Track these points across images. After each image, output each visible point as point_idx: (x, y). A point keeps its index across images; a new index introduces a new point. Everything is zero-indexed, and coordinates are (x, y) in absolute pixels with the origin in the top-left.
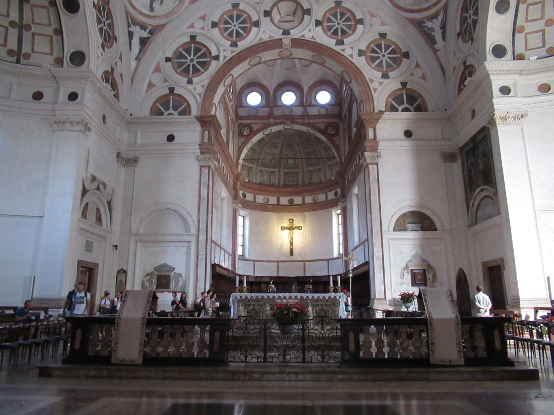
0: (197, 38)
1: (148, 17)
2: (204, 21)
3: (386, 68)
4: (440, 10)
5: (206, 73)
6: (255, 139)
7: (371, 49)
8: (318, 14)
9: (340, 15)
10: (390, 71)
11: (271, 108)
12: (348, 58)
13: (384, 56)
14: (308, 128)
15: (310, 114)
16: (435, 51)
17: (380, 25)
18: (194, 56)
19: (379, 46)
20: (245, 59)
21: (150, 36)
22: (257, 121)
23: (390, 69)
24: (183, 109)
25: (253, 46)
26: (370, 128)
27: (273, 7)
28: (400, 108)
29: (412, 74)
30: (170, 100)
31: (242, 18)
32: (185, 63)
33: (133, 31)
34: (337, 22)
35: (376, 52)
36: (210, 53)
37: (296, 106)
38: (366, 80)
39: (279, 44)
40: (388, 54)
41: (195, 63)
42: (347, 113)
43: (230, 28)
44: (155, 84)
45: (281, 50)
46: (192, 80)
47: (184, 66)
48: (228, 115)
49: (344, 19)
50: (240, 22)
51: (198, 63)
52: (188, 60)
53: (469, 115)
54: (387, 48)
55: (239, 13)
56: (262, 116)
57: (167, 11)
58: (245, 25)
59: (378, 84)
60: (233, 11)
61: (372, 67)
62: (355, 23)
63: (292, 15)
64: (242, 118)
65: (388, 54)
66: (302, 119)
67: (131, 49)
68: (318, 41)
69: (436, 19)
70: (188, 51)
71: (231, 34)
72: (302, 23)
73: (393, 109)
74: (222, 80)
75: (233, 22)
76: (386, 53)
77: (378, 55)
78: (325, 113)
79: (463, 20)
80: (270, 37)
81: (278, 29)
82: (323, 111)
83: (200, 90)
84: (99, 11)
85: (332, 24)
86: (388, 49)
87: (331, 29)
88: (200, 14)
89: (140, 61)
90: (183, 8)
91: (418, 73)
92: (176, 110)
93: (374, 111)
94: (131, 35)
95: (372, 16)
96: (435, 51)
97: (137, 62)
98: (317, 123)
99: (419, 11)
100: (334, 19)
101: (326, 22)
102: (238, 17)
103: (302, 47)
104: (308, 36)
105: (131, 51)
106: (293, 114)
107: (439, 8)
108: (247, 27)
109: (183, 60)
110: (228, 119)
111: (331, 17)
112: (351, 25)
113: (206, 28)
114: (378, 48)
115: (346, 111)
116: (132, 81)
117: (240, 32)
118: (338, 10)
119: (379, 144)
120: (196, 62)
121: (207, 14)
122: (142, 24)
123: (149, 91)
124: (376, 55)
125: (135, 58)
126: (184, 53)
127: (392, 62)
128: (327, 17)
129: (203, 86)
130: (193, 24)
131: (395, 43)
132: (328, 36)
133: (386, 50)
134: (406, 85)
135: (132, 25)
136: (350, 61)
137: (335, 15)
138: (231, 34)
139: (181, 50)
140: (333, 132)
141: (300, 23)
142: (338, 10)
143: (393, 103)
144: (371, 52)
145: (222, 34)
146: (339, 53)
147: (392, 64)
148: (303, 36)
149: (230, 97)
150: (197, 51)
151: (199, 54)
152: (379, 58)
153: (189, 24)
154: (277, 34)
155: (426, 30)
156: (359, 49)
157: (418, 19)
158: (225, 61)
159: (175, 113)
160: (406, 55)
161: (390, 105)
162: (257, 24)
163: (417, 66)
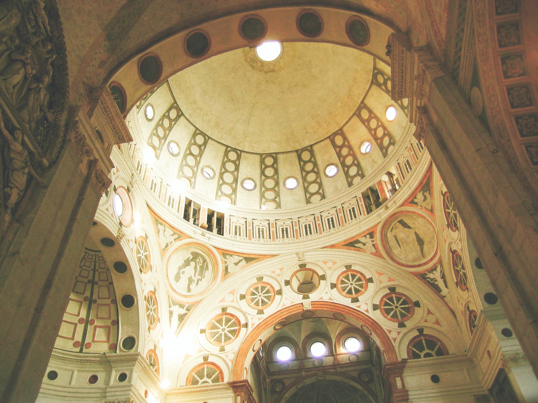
1: (186, 296)
2: (233, 295)
4: (436, 264)
6: (287, 395)
7: (384, 302)
8: (333, 278)
12: (364, 314)
13: (397, 307)
14: (341, 378)
16: (442, 298)
18: (225, 326)
19: (391, 299)
22: (289, 376)
23: (405, 318)
24: (216, 376)
26: (397, 377)
27: (292, 277)
28: (422, 354)
29: (426, 321)
31: (266, 289)
33: (172, 310)
36: (239, 322)
40: (400, 305)
41: (226, 332)
43: (256, 298)
47: (217, 336)
49: (355, 279)
53: (486, 355)
54: (398, 299)
55: (263, 285)
56: (293, 370)
58: (269, 294)
59: (397, 334)
60: (258, 284)
61: (388, 319)
64: (273, 374)
65: (400, 305)
66: (334, 369)
73: (416, 356)
76: (399, 304)
77: (392, 307)
78: (356, 360)
79: (457, 272)
83: (232, 356)
84: (148, 301)
85: (346, 285)
86: (400, 301)
87: (346, 289)
92: (210, 378)
94: (171, 313)
96: (442, 298)
98: (349, 371)
99: (420, 266)
100: (346, 281)
102: (263, 288)
108: (270, 296)
110: (260, 377)
111: (344, 279)
112: (362, 284)
113: (235, 300)
119: (410, 393)
122: (181, 303)
124: (389, 307)
126: (216, 323)
127: (406, 312)
128: (340, 280)
134: (423, 332)
140: (367, 379)
143: (414, 350)
144: (384, 306)
147: (406, 313)
148: (321, 298)
149: (260, 356)
150: (228, 321)
151: (230, 323)
152: (393, 309)
156: (373, 304)
157: (420, 272)
159: (209, 380)
160: (417, 304)
162: (280, 292)
163: (429, 312)
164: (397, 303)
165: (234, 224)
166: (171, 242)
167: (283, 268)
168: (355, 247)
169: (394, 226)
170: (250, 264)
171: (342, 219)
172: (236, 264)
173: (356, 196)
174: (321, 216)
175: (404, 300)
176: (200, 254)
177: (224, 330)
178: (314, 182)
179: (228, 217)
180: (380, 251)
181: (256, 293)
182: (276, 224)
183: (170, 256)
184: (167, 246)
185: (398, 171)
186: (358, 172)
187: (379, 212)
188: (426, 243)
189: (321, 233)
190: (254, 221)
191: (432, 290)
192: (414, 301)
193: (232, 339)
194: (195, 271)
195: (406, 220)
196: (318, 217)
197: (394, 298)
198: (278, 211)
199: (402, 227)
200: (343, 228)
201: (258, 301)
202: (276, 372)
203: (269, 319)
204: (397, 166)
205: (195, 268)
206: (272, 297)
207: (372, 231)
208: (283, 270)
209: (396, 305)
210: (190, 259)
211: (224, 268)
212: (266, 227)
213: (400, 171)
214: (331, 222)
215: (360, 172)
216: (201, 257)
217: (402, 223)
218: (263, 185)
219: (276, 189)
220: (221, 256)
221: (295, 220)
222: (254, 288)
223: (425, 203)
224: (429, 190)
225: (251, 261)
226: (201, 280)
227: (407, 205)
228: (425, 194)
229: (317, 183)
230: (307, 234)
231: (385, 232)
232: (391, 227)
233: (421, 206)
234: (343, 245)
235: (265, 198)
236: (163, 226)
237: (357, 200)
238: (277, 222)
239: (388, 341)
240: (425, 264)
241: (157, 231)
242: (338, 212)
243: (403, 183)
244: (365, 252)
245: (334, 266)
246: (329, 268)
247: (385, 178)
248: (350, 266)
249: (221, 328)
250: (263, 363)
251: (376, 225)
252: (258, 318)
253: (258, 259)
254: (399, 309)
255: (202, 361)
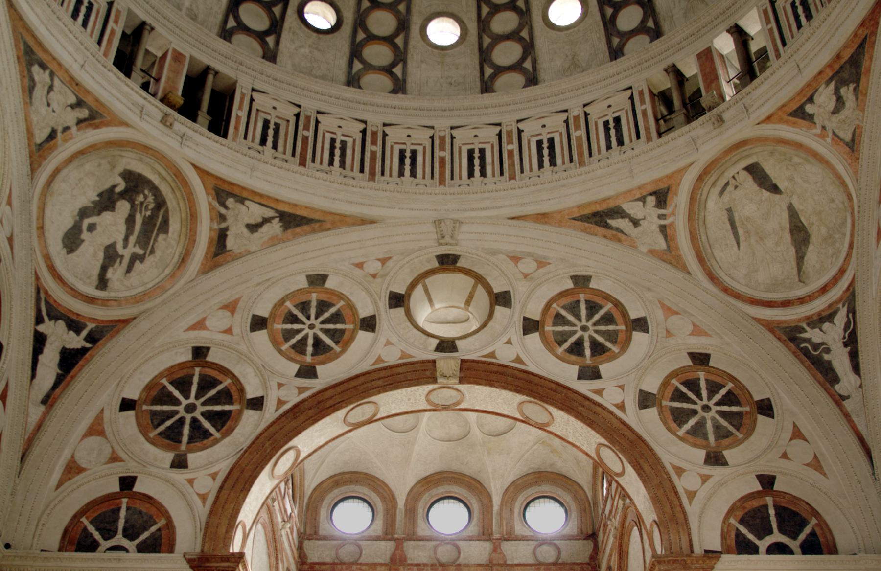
0: (211, 353)
1: (91, 300)
3: (717, 439)
5: (227, 440)
7: (673, 389)
9: (587, 308)
10: (728, 447)
11: (399, 542)
12: (612, 413)
13: (706, 408)
15: (509, 562)
17: (692, 334)
18: (197, 398)
19: (692, 384)
20: (335, 408)
21: (88, 345)
23: (725, 442)
24: (152, 535)
25: (357, 377)
27: (413, 286)
28: (763, 544)
29: (785, 456)
30: (119, 509)
31: (333, 310)
32: (170, 415)
33: (46, 332)
34: (579, 325)
35: (688, 400)
36: (242, 390)
37: (471, 539)
38: (663, 467)
39: (428, 373)
40: (718, 404)
42: (615, 558)
43: (298, 331)
44: (84, 466)
45: (431, 387)
46: (187, 457)
47: (168, 423)
48: (277, 559)
49: (596, 317)
50: (328, 318)
51: (207, 415)
52: (181, 408)
54: (714, 388)
55: (324, 297)
57: (141, 289)
58: (339, 326)
60: (310, 292)
61: (678, 437)
62: (626, 327)
63: (462, 305)
65: (718, 404)
67: (33, 376)
68: (532, 368)
69: (830, 322)
70: (183, 385)
71: (300, 348)
72: (490, 324)
73: (745, 547)
74: (271, 458)
75: (309, 318)
80: (404, 355)
81: (424, 337)
82: (548, 554)
83: (208, 485)
85: (567, 328)
86: (717, 392)
87: (566, 341)
88: (226, 297)
89: (52, 406)
90: (182, 282)
91: (801, 452)
93: (692, 551)
94: (40, 341)
95: (669, 311)
96: (839, 400)
97: (46, 408)
99: (786, 304)
100: (570, 318)
101: (551, 323)
102: (323, 306)
103: (489, 382)
104: (505, 356)
105: (34, 380)
106: (461, 560)
107: (835, 298)
108: (342, 331)
109: (166, 408)
112: (616, 332)
113: (236, 330)
114: (690, 390)
115: (611, 555)
116: (23, 457)
117: (323, 342)
118: (582, 297)
120: (203, 414)
121: (240, 298)
122: (74, 317)
123: (67, 484)
124: (685, 405)
125: (41, 397)
126: (171, 388)
127: (731, 423)
129: (214, 476)
130: (204, 319)
131: (732, 379)
132: (557, 356)
133: (712, 391)
135: (46, 318)
136: (620, 420)
137: (573, 308)
138: (300, 348)
139: (164, 381)
141: (484, 326)
142: (582, 297)
143: (743, 530)
144: (672, 399)
145: (276, 344)
146: (587, 398)
148: (492, 355)
149: (286, 511)
150: (207, 384)
151: (212, 393)
152: (695, 412)
153: (193, 319)
154: (424, 351)
155: (810, 348)
156: (641, 392)
157: (785, 322)
158: (282, 411)
160: (765, 408)
161: (733, 534)
162: (369, 324)
163: (797, 434)
164: (709, 399)
165: (262, 116)
166: (66, 129)
167: (390, 258)
168: (607, 226)
169: (732, 182)
170: (295, 236)
171: (580, 146)
172: (253, 228)
173: (631, 88)
174: (520, 132)
175: (729, 393)
176: (149, 182)
177: (190, 408)
178: (513, 36)
179: (248, 92)
180: (677, 248)
181: (301, 316)
182: (385, 135)
183: (57, 171)
184: (52, 136)
185: (768, 22)
186: (644, 21)
187: (693, 133)
188: (815, 239)
189: (512, 177)
190: (321, 118)
191: (814, 376)
192: (757, 398)
193: (212, 438)
194: (128, 229)
195: (770, 168)
196: (509, 134)
197: (703, 384)
198: (398, 100)
199: (755, 187)
200: (583, 169)
201: (304, 341)
202: (324, 564)
203: (330, 393)
204: (765, 12)
205: (130, 221)
206: (346, 336)
207: (666, 186)
208: (390, 264)
209: (705, 402)
210: (118, 190)
211: (215, 236)
212: (354, 141)
213: (773, 24)
214: (546, 152)
215: (650, 24)
216: (150, 190)
217: (754, 171)
218: (360, 22)
219: (399, 41)
220: (210, 199)
221: (442, 134)
222: (297, 302)
223: (835, 119)
224: (857, 81)
225: (298, 225)
226: (142, 258)
227: (781, 121)
228: (843, 91)
229: (521, 40)
230: (471, 174)
231: (701, 195)
232: (721, 183)
233: (824, 128)
234: (574, 219)
235: (362, 61)
236: (48, 72)
237: (631, 98)
238: (387, 130)
239: (672, 496)
240: (802, 301)
241: (26, 81)
242: (572, 127)
243: (778, 56)
244: (634, 246)
245: (541, 270)
246: (526, 276)
247: (725, 44)
248: (587, 279)
249: (185, 402)
250: (292, 533)
251: (682, 171)
252: (299, 388)
253: (317, 225)
254: (712, 413)
255: (116, 488)
